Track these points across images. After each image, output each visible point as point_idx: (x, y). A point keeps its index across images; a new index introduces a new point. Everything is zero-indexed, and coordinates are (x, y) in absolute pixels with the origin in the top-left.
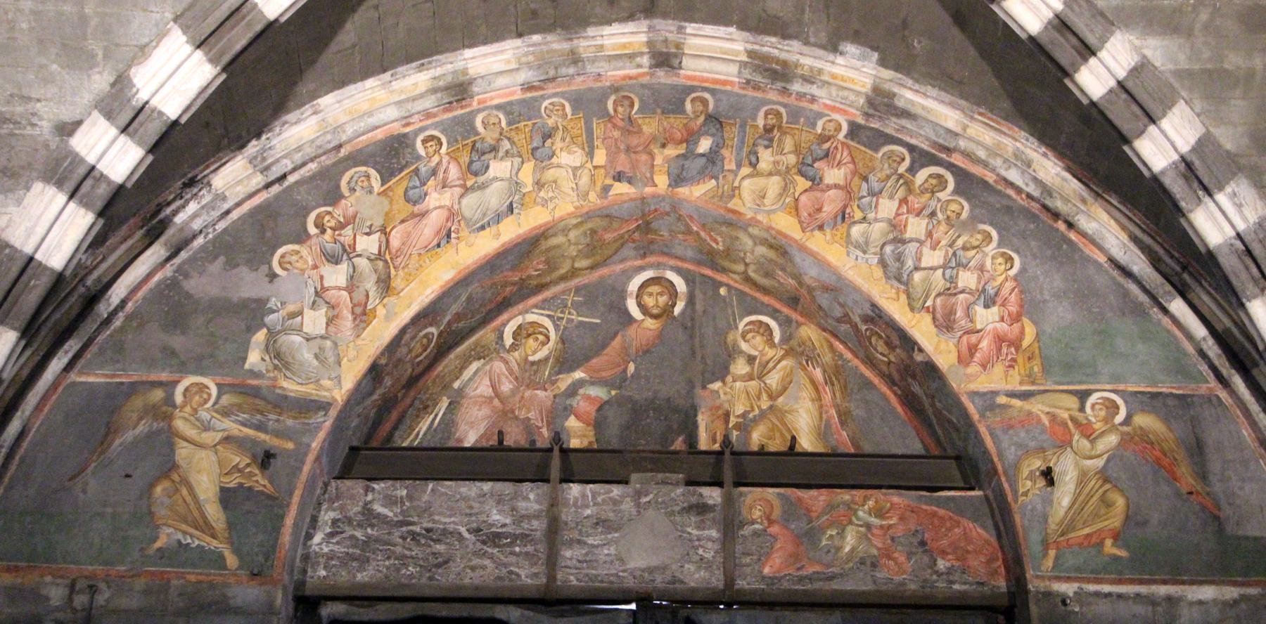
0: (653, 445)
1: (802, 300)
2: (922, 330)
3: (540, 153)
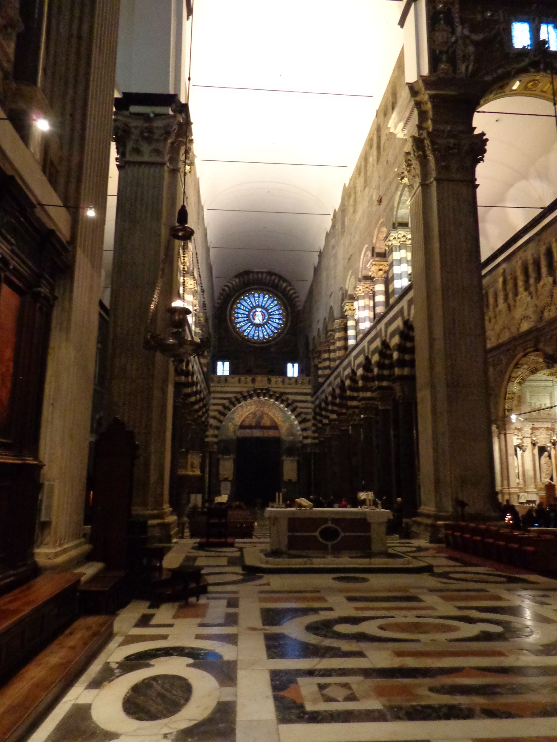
0: (259, 426)
1: (268, 415)
2: (276, 420)
3: (251, 406)
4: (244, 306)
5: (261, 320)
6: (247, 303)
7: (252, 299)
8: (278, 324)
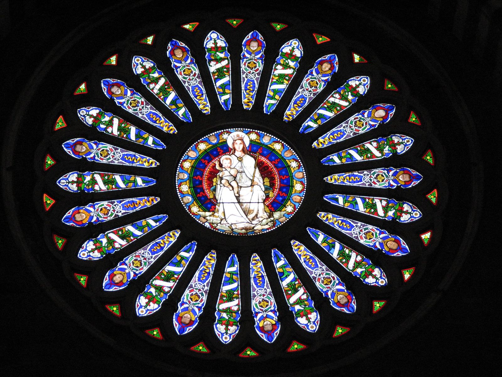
4: (129, 118)
5: (260, 209)
6: (151, 99)
7: (187, 71)
8: (391, 226)
